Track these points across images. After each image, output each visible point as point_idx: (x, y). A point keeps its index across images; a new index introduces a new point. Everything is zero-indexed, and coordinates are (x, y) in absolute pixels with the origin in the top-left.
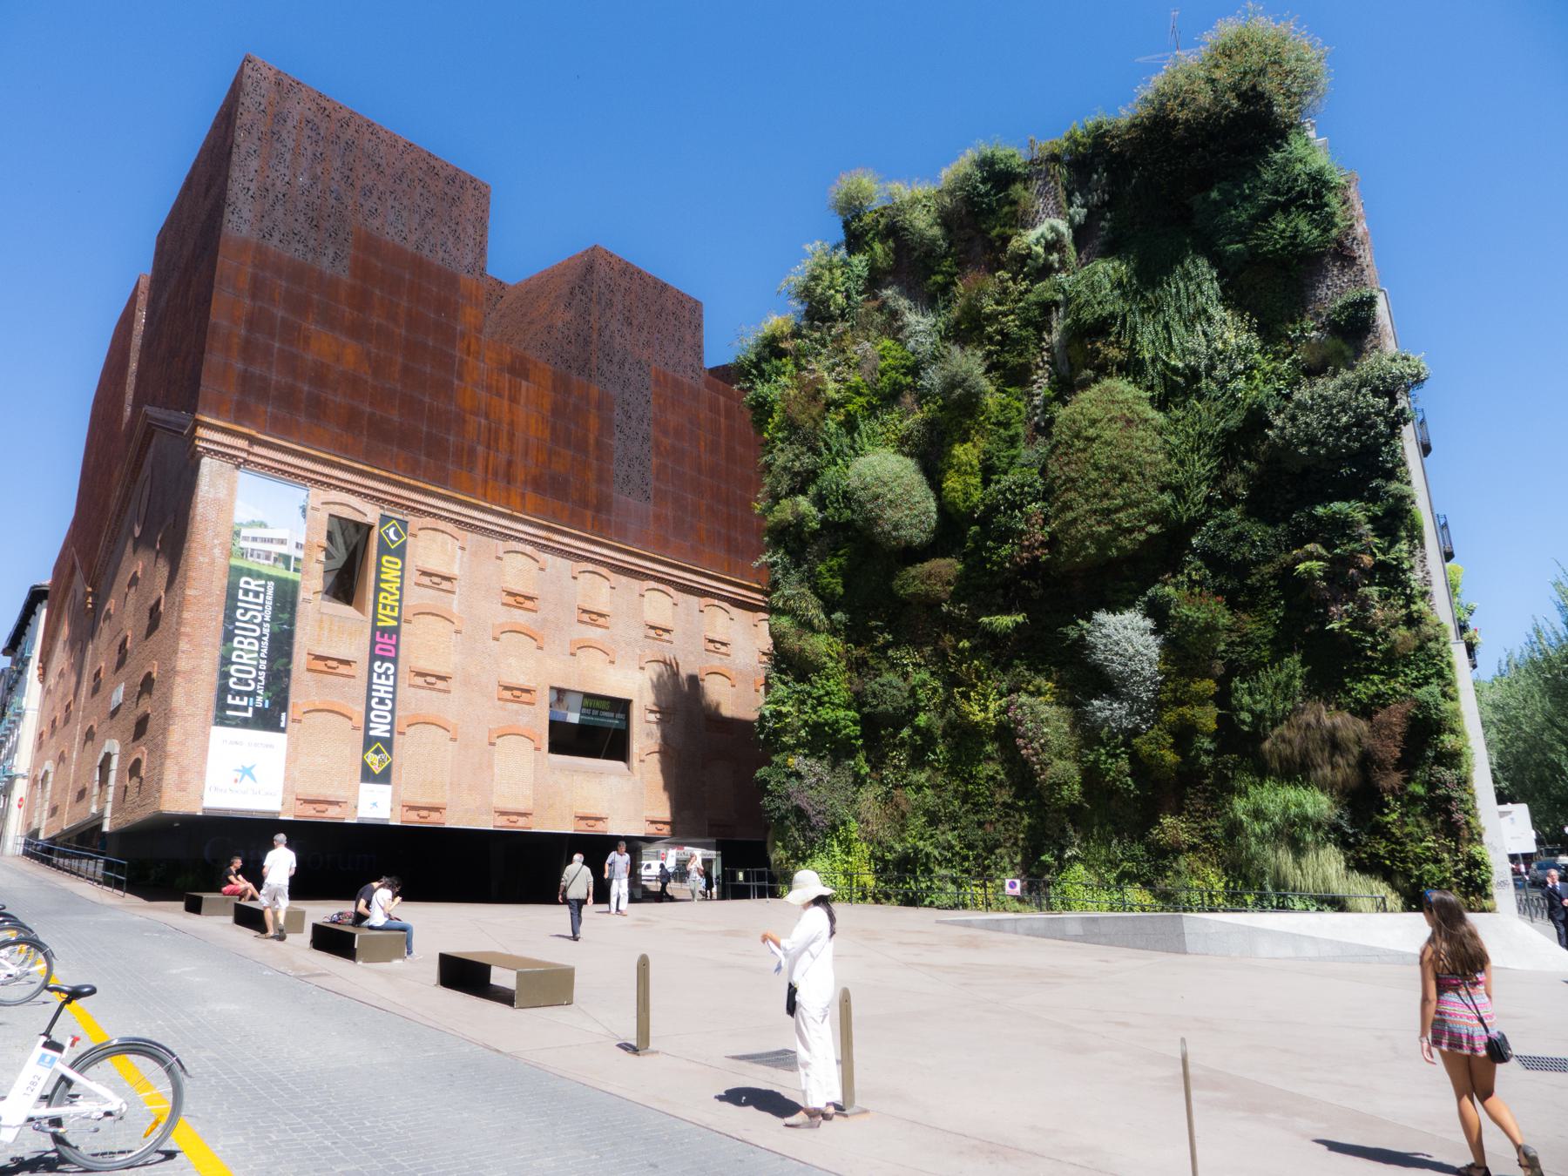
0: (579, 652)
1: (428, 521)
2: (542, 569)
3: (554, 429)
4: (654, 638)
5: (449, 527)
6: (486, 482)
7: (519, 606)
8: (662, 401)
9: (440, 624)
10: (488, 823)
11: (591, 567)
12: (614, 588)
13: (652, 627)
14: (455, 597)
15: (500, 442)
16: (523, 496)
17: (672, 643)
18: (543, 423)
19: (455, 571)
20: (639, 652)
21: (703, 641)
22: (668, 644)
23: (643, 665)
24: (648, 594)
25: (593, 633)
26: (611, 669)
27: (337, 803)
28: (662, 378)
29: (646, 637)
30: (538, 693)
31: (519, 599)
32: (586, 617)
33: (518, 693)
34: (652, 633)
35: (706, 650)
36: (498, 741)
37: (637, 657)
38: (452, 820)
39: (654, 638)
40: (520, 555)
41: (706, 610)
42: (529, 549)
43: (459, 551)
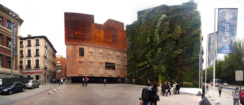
1: (90, 47)
5: (92, 47)
6: (96, 42)
10: (98, 76)
11: (110, 50)
19: (93, 51)
25: (110, 57)
27: (83, 74)
31: (101, 54)
32: (109, 55)
33: (101, 63)
34: (118, 56)
36: (99, 68)
38: (95, 76)
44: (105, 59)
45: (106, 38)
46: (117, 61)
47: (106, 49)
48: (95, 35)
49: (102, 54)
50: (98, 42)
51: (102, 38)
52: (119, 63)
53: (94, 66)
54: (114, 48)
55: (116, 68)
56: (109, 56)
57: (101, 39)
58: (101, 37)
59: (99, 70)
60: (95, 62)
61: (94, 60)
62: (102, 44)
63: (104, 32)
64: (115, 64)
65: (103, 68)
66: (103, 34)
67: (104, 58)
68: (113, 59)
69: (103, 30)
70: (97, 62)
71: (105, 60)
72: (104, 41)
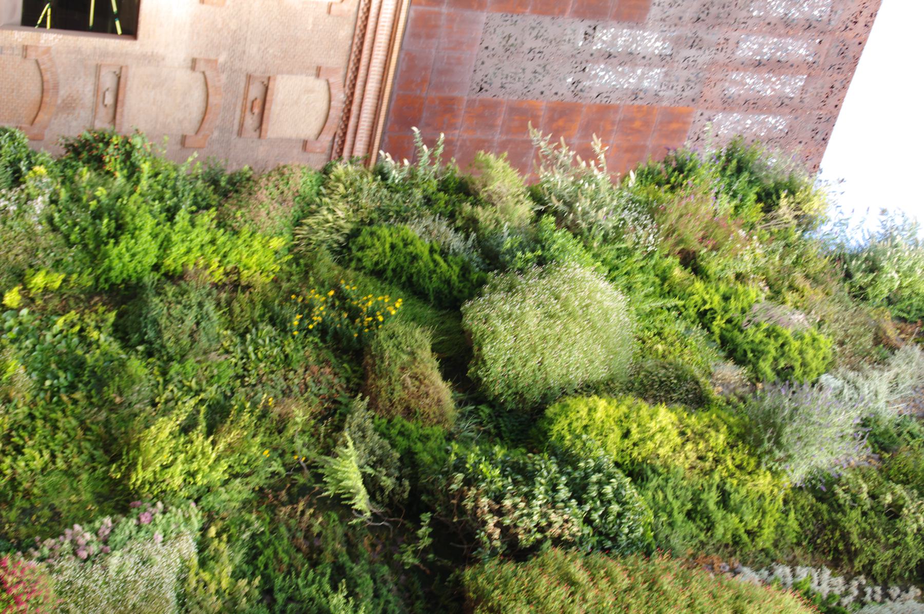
4: (245, 98)
8: (637, 124)
12: (329, 12)
13: (267, 89)
17: (240, 133)
20: (222, 59)
22: (236, 127)
23: (201, 66)
24: (321, 85)
28: (674, 126)
29: (249, 78)
34: (255, 92)
37: (213, 57)
39: (245, 98)
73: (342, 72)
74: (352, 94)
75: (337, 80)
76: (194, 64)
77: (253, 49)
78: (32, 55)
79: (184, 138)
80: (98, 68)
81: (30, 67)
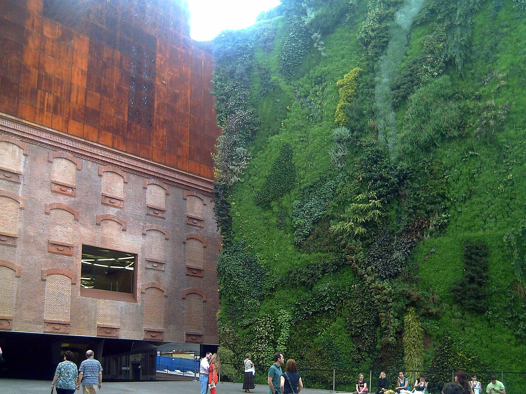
0: (102, 224)
2: (79, 170)
3: (89, 78)
6: (42, 111)
7: (62, 193)
8: (162, 63)
9: (11, 205)
11: (111, 168)
14: (21, 186)
15: (53, 87)
16: (67, 122)
17: (164, 219)
18: (82, 74)
19: (21, 169)
20: (142, 224)
21: (186, 219)
22: (163, 220)
23: (145, 232)
24: (149, 188)
25: (112, 212)
26: (123, 234)
30: (75, 249)
32: (107, 201)
34: (151, 212)
35: (187, 224)
36: (48, 278)
37: (142, 227)
40: (64, 159)
41: (188, 198)
42: (70, 155)
43: (23, 157)
44: (84, 226)
45: (99, 95)
46: (148, 239)
47: (90, 165)
48: (40, 67)
49: (70, 191)
50: (55, 111)
51: (75, 87)
52: (157, 254)
53: (17, 264)
54: (134, 163)
55: (139, 285)
56: (105, 207)
57: (73, 99)
58: (71, 84)
59: (46, 289)
60: (28, 240)
61: (20, 225)
62: (74, 126)
63: (90, 52)
64: (135, 255)
65: (69, 282)
66: (82, 64)
67: (76, 220)
68: (124, 230)
69: (87, 39)
70: (39, 239)
71: (82, 229)
72: (86, 109)
73: (145, 179)
74: (152, 175)
75: (148, 181)
76: (144, 234)
77: (139, 212)
78: (144, 291)
79: (166, 239)
80: (146, 268)
81: (147, 292)
